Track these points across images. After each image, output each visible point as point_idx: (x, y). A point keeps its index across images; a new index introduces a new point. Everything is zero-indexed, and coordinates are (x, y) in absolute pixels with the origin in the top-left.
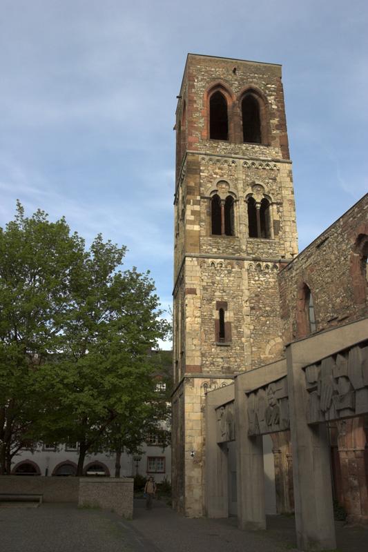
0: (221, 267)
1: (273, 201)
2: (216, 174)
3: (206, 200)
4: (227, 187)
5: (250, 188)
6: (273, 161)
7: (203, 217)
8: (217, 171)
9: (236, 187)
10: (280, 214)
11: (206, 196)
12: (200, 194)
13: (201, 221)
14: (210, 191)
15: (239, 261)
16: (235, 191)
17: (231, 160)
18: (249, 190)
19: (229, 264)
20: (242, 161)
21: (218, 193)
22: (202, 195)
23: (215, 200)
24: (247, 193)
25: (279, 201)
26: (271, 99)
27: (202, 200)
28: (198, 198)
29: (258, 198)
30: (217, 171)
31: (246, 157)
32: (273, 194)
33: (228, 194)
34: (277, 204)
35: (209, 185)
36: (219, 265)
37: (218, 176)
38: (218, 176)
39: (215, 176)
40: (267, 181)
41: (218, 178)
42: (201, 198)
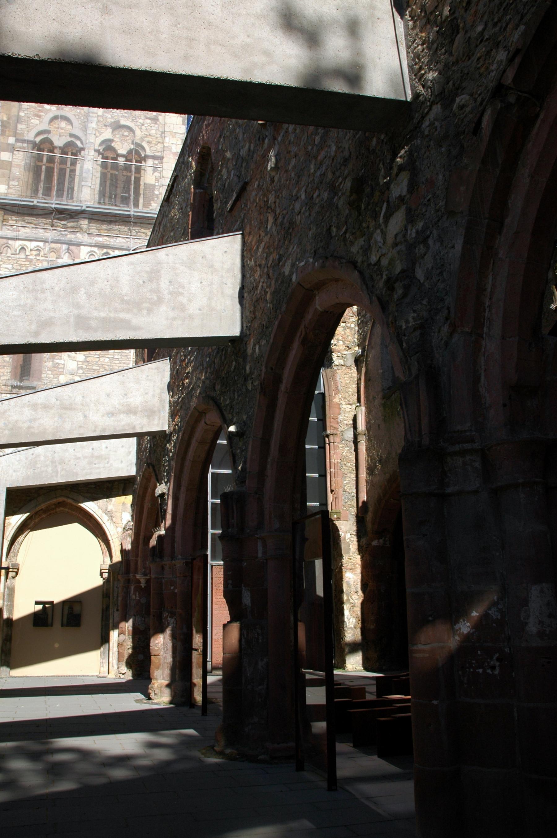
0: (39, 255)
1: (148, 152)
3: (25, 145)
4: (70, 127)
5: (110, 130)
7: (16, 172)
9: (85, 129)
10: (157, 174)
11: (26, 138)
12: (15, 134)
15: (72, 248)
16: (80, 134)
18: (107, 134)
19: (52, 250)
21: (49, 136)
22: (21, 138)
24: (102, 138)
25: (158, 154)
27: (19, 144)
29: (122, 149)
32: (149, 142)
33: (70, 139)
34: (154, 158)
35: (35, 121)
36: (34, 253)
40: (141, 121)
42: (17, 141)
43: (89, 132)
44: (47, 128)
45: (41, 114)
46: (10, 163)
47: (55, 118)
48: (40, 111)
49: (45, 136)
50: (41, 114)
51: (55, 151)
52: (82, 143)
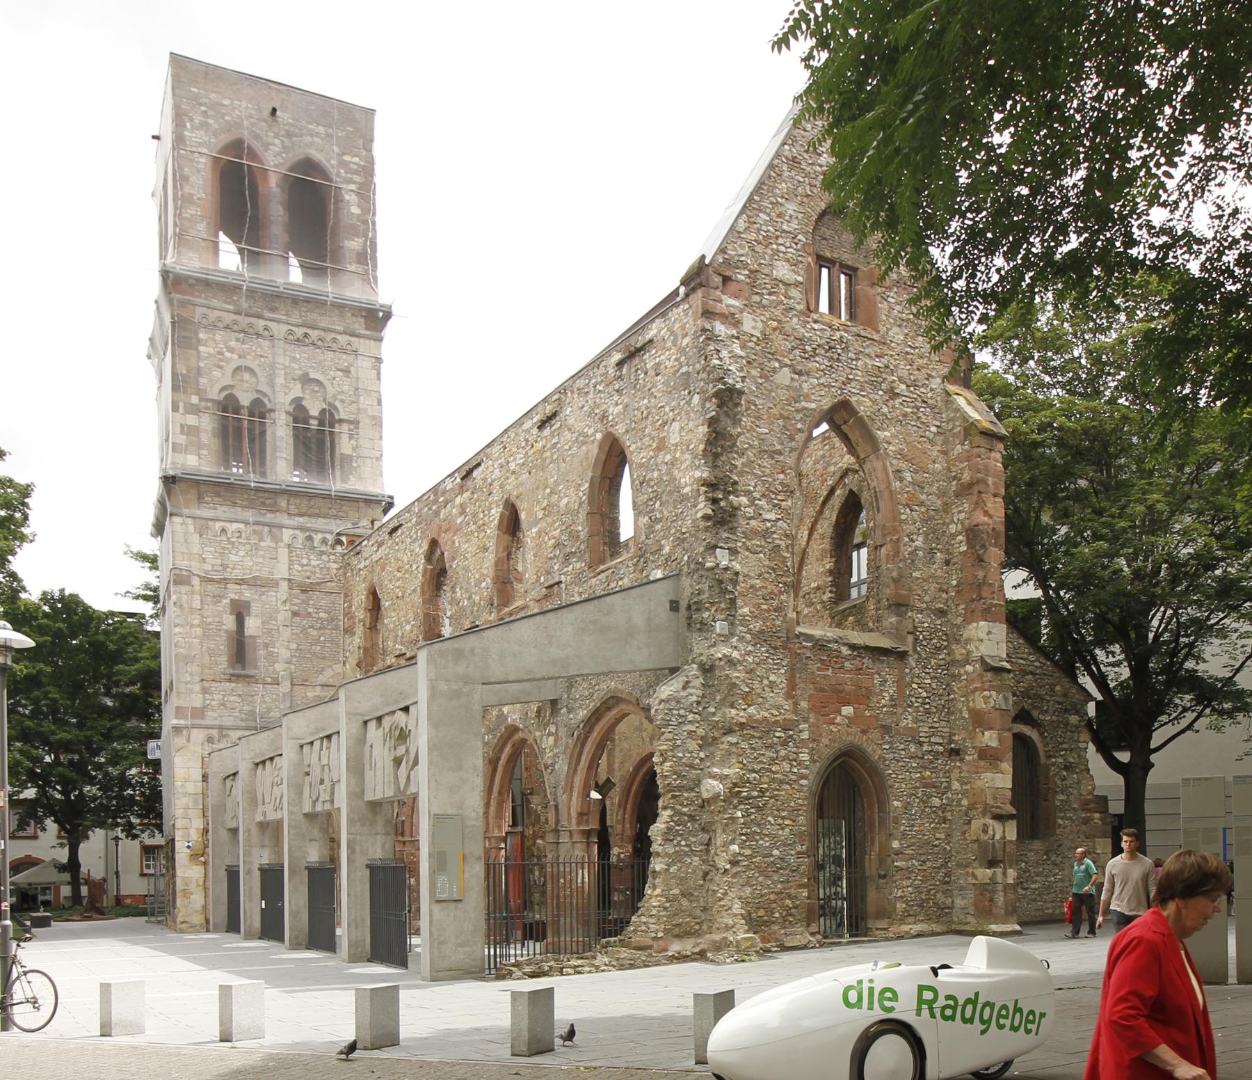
2: (231, 350)
3: (210, 404)
4: (254, 380)
6: (345, 333)
8: (233, 344)
12: (199, 392)
13: (200, 446)
14: (218, 387)
17: (261, 323)
20: (285, 328)
21: (234, 392)
23: (228, 406)
26: (350, 198)
27: (203, 404)
28: (195, 399)
30: (233, 344)
31: (292, 320)
35: (217, 373)
37: (235, 356)
38: (235, 356)
39: (228, 355)
41: (234, 359)
43: (277, 389)
44: (232, 383)
45: (222, 364)
46: (198, 427)
47: (238, 369)
48: (221, 360)
49: (229, 392)
50: (222, 364)
51: (242, 412)
52: (269, 400)
